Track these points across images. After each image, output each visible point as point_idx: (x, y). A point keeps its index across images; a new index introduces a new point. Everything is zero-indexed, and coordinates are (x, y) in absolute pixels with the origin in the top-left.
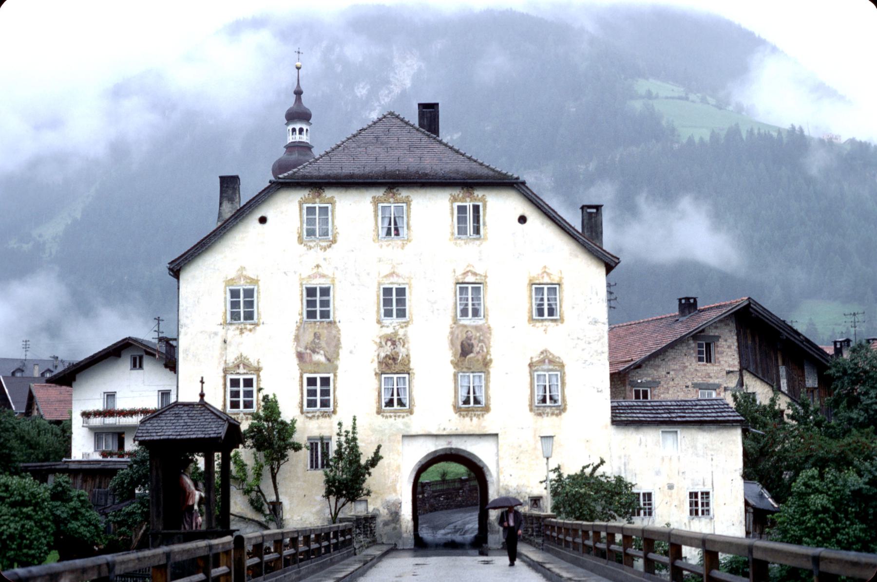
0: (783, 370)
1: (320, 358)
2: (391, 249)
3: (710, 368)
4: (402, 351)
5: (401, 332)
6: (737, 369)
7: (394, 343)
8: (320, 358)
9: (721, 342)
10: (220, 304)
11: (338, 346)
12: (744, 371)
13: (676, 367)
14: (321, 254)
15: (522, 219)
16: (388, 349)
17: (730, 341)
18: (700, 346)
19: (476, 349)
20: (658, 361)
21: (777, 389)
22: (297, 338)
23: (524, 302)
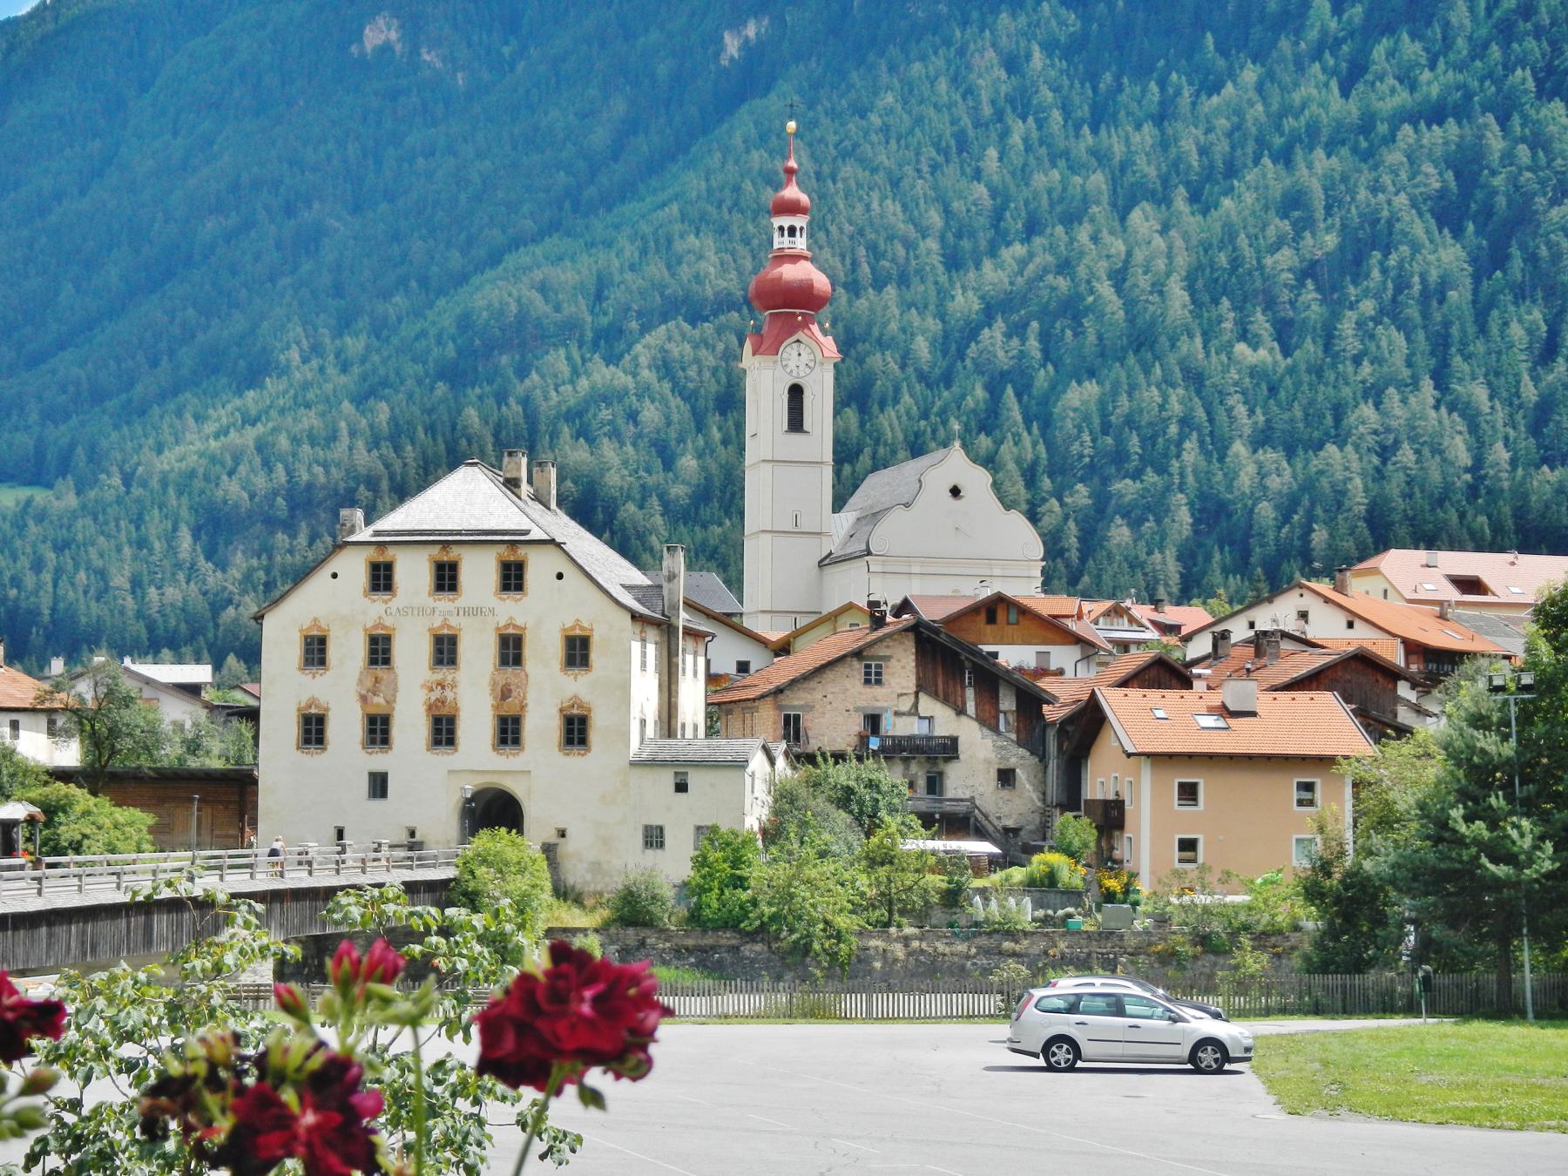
0: (970, 693)
1: (379, 700)
2: (445, 603)
3: (877, 691)
4: (449, 694)
5: (449, 678)
6: (913, 689)
7: (443, 687)
8: (379, 700)
9: (893, 662)
10: (296, 652)
11: (396, 690)
12: (921, 695)
13: (836, 690)
14: (384, 606)
15: (560, 576)
16: (437, 694)
17: (904, 661)
18: (868, 666)
19: (514, 694)
20: (813, 684)
21: (961, 711)
22: (360, 681)
23: (557, 650)
